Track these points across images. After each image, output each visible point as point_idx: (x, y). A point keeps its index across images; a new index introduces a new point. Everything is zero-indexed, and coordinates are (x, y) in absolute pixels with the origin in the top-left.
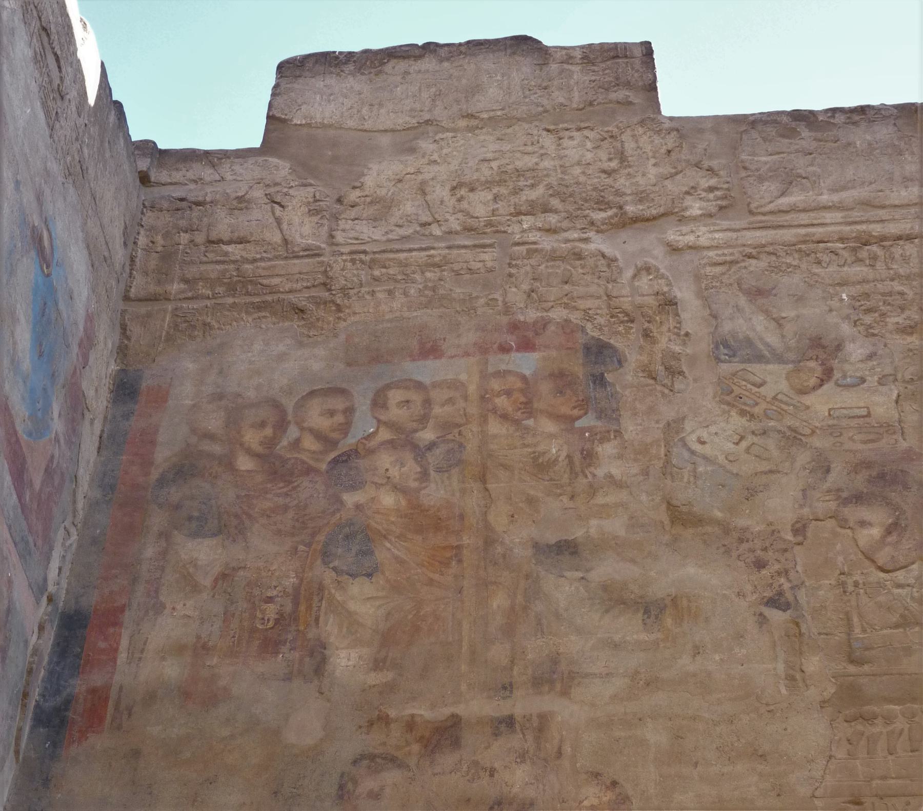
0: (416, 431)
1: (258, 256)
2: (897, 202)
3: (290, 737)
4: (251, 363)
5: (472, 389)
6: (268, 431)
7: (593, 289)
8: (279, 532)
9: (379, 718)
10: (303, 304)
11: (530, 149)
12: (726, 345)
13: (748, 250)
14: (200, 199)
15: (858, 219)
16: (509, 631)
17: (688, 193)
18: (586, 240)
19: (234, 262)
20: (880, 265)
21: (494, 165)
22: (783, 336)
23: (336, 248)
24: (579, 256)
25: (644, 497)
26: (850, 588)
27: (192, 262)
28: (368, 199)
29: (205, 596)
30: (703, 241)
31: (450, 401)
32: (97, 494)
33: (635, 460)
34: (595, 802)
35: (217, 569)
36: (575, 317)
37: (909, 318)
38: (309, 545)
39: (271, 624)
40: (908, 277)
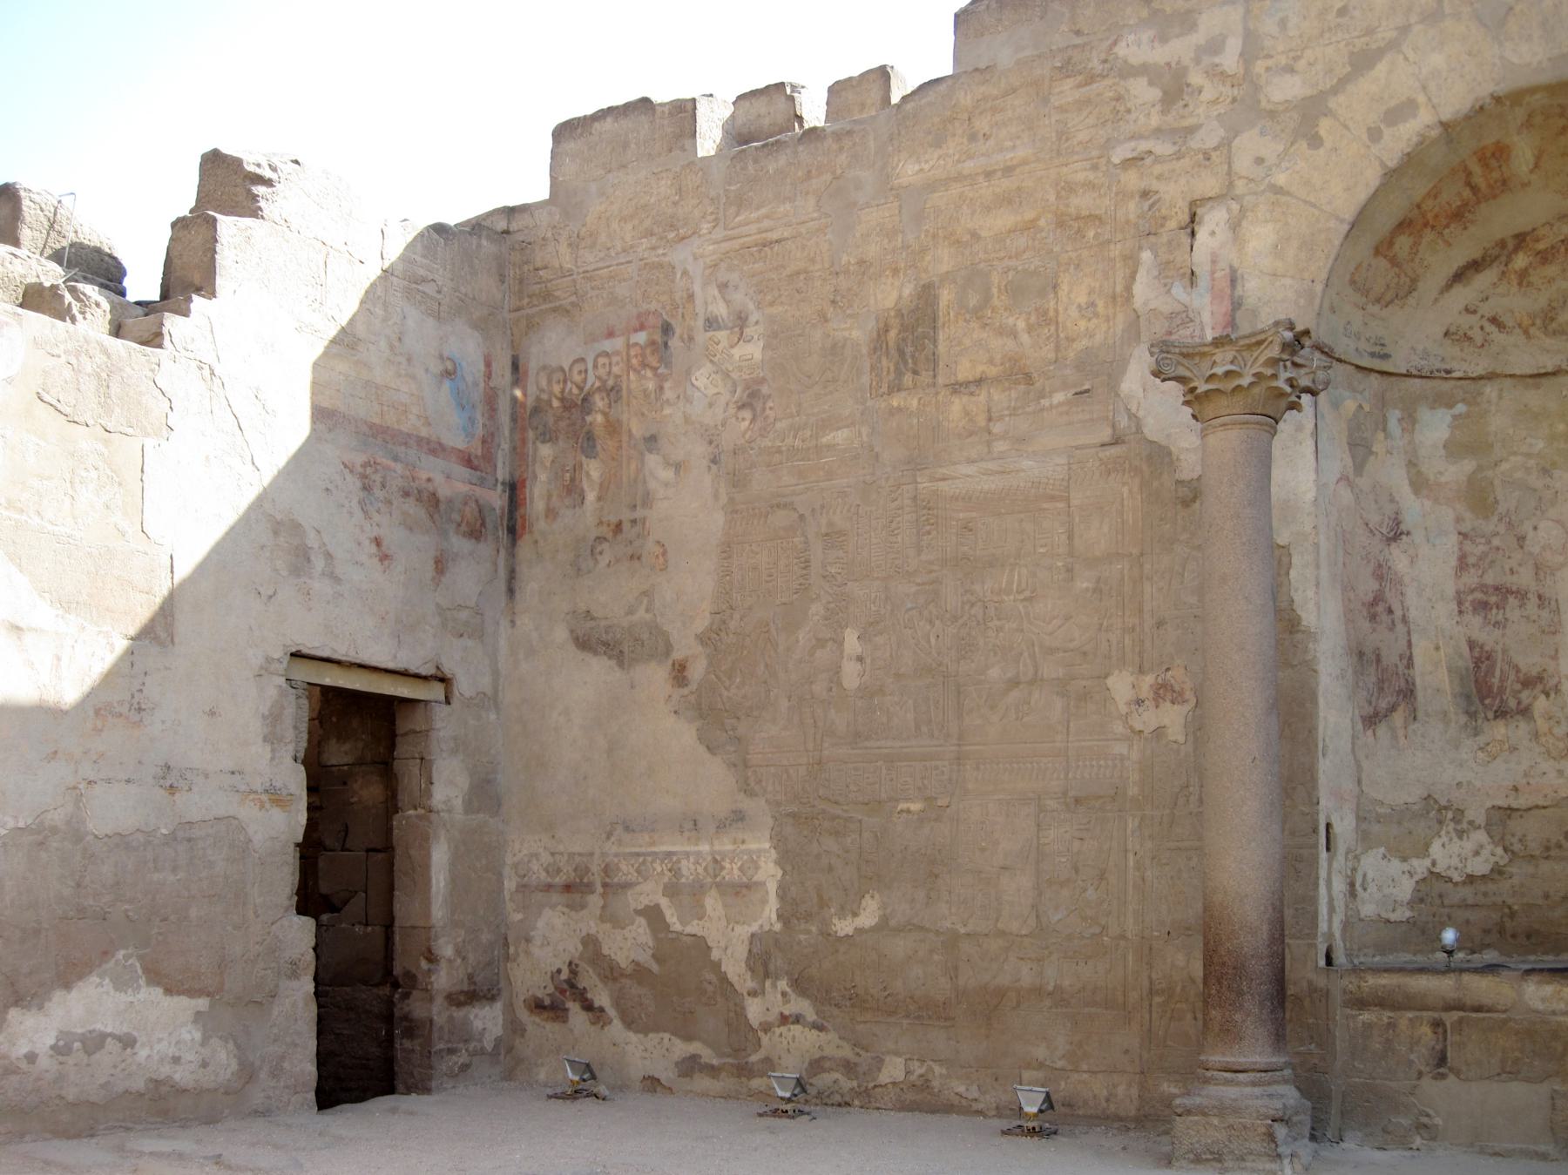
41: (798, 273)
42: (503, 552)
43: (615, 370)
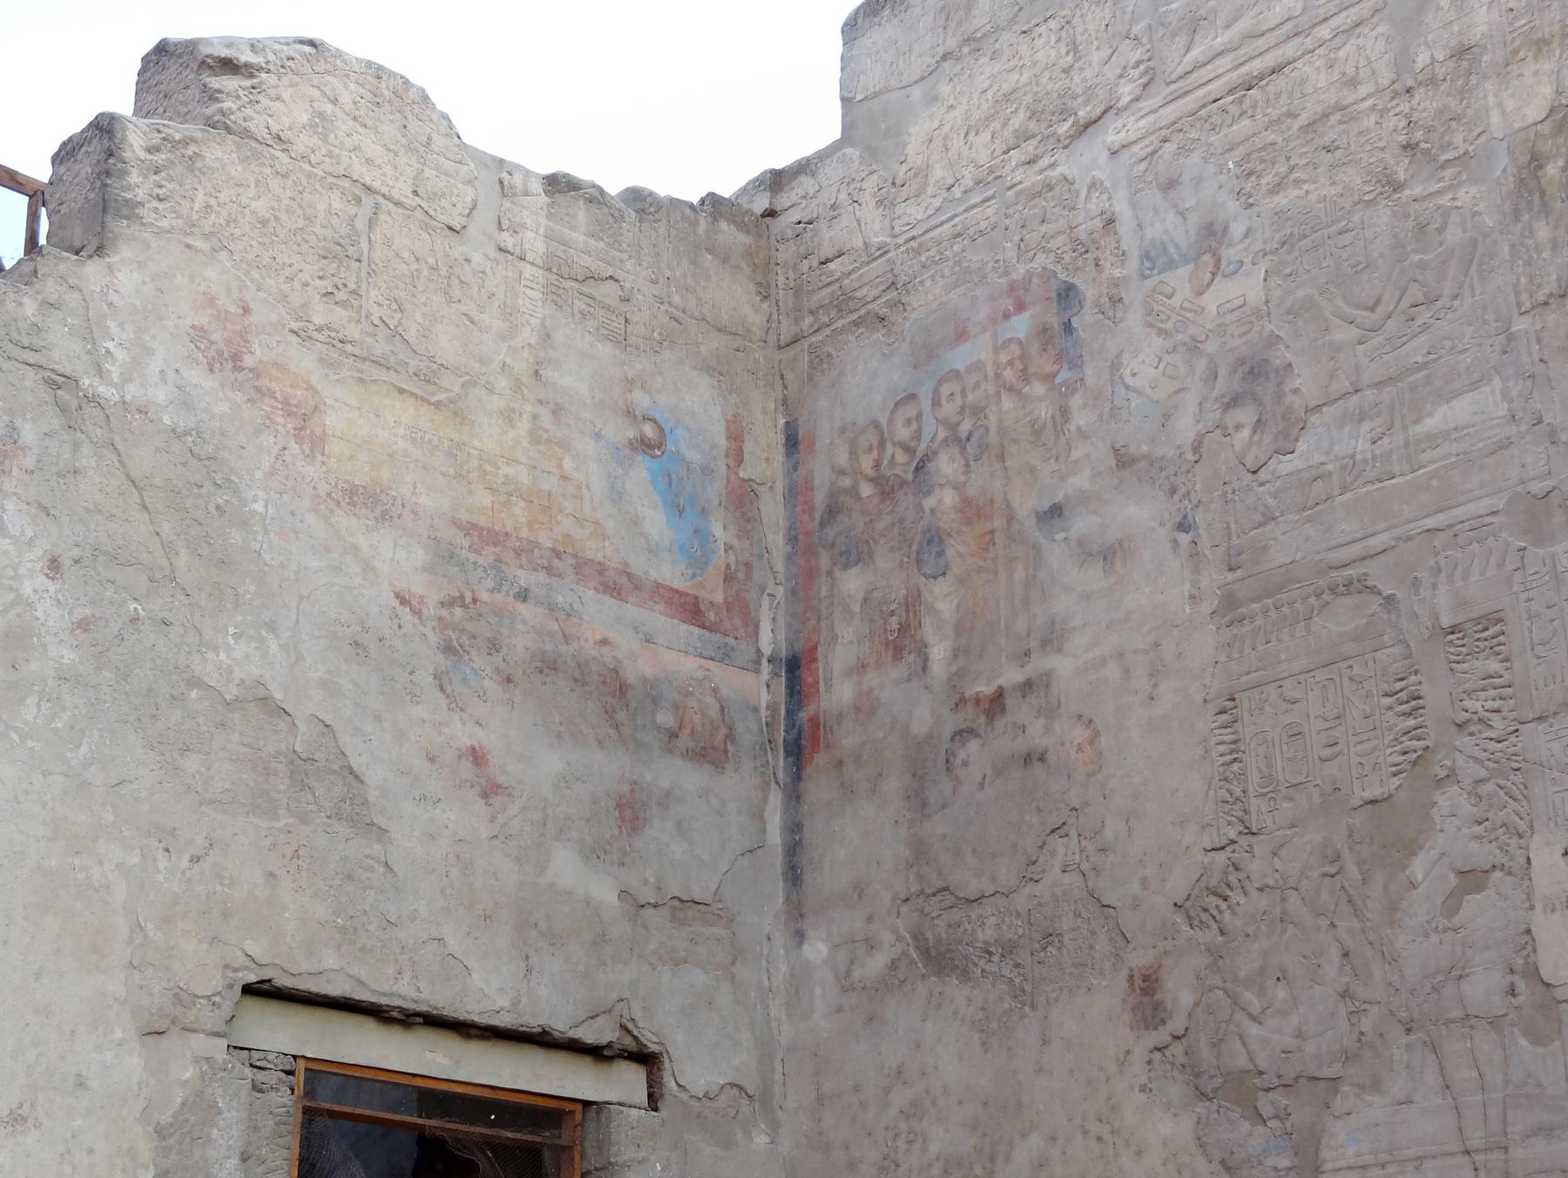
2: (1272, 24)
6: (875, 454)
13: (1164, 133)
16: (1026, 602)
17: (1121, 76)
18: (1053, 166)
21: (989, 94)
26: (1230, 496)
30: (1133, 136)
32: (789, 548)
34: (1078, 740)
35: (861, 597)
37: (1277, 174)
40: (1278, 121)
41: (1325, 116)
42: (776, 799)
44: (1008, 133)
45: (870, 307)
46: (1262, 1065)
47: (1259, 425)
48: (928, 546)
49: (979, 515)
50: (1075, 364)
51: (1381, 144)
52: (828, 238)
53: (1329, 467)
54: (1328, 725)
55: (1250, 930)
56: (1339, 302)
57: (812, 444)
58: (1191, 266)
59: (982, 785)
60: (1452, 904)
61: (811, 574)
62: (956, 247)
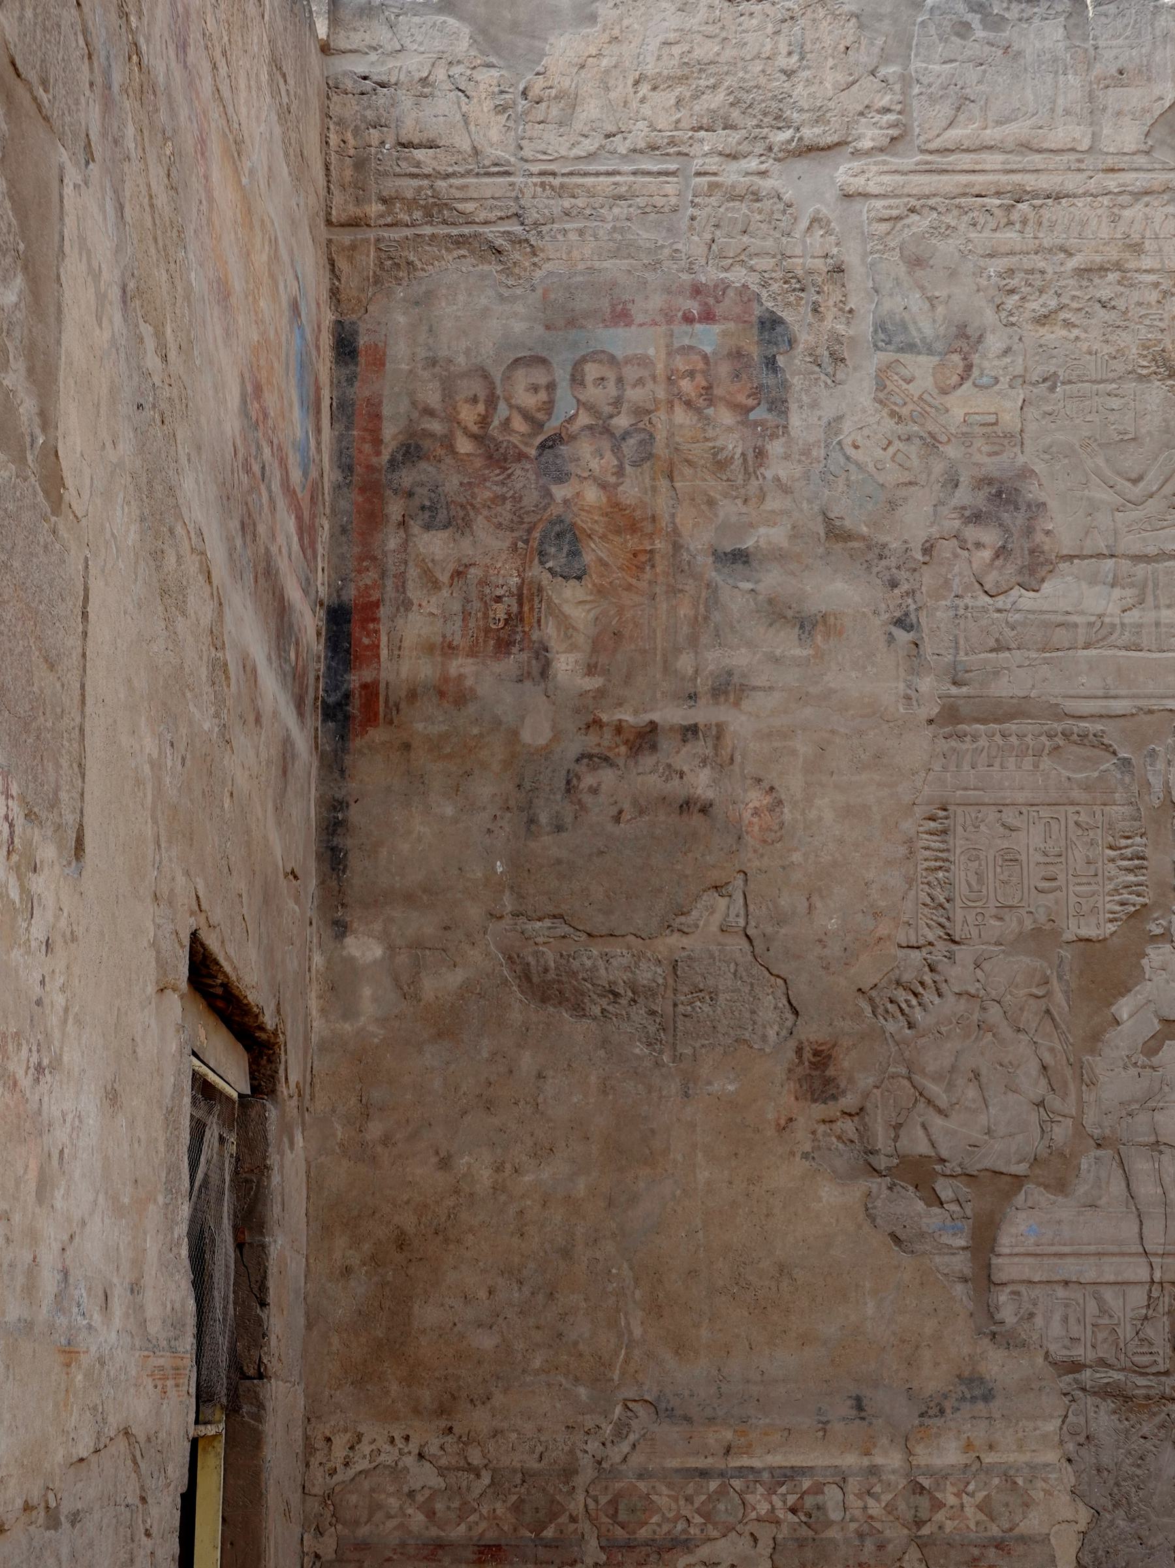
0: (611, 417)
1: (450, 170)
2: (1053, 146)
3: (526, 736)
4: (457, 318)
5: (660, 367)
6: (481, 408)
7: (769, 243)
8: (499, 526)
9: (595, 722)
10: (499, 242)
11: (710, 29)
12: (884, 330)
13: (913, 202)
14: (384, 78)
15: (1015, 167)
16: (693, 641)
17: (861, 114)
18: (763, 174)
19: (427, 176)
20: (1029, 232)
21: (676, 50)
22: (934, 321)
23: (527, 166)
24: (757, 197)
25: (805, 505)
26: (961, 612)
27: (386, 174)
28: (553, 92)
29: (445, 593)
30: (872, 188)
31: (640, 382)
33: (799, 461)
34: (757, 804)
35: (451, 567)
36: (753, 281)
38: (526, 542)
39: (501, 625)
41: (1103, 270)
43: (634, 395)
44: (699, 107)
45: (481, 229)
46: (944, 1154)
47: (1002, 552)
48: (556, 541)
49: (634, 527)
50: (779, 405)
51: (1161, 324)
52: (413, 118)
53: (1074, 618)
54: (1048, 860)
55: (943, 1029)
56: (1102, 464)
57: (379, 362)
58: (935, 359)
59: (617, 819)
60: (1152, 1047)
61: (373, 518)
62: (616, 210)
